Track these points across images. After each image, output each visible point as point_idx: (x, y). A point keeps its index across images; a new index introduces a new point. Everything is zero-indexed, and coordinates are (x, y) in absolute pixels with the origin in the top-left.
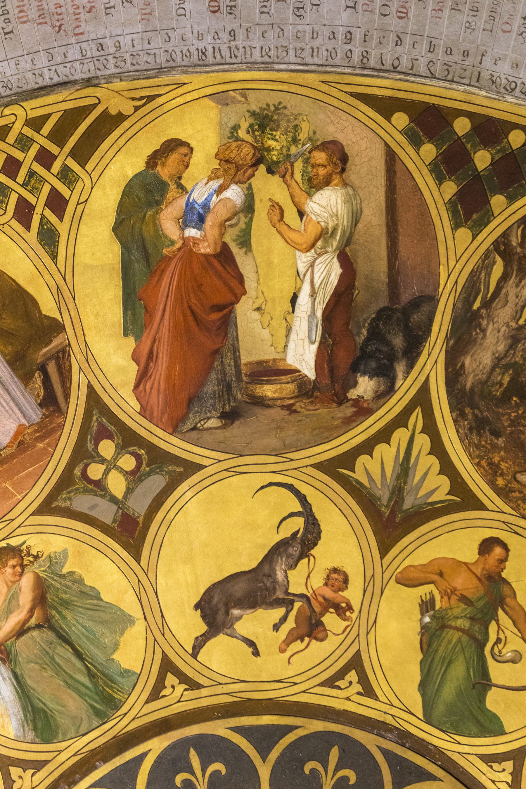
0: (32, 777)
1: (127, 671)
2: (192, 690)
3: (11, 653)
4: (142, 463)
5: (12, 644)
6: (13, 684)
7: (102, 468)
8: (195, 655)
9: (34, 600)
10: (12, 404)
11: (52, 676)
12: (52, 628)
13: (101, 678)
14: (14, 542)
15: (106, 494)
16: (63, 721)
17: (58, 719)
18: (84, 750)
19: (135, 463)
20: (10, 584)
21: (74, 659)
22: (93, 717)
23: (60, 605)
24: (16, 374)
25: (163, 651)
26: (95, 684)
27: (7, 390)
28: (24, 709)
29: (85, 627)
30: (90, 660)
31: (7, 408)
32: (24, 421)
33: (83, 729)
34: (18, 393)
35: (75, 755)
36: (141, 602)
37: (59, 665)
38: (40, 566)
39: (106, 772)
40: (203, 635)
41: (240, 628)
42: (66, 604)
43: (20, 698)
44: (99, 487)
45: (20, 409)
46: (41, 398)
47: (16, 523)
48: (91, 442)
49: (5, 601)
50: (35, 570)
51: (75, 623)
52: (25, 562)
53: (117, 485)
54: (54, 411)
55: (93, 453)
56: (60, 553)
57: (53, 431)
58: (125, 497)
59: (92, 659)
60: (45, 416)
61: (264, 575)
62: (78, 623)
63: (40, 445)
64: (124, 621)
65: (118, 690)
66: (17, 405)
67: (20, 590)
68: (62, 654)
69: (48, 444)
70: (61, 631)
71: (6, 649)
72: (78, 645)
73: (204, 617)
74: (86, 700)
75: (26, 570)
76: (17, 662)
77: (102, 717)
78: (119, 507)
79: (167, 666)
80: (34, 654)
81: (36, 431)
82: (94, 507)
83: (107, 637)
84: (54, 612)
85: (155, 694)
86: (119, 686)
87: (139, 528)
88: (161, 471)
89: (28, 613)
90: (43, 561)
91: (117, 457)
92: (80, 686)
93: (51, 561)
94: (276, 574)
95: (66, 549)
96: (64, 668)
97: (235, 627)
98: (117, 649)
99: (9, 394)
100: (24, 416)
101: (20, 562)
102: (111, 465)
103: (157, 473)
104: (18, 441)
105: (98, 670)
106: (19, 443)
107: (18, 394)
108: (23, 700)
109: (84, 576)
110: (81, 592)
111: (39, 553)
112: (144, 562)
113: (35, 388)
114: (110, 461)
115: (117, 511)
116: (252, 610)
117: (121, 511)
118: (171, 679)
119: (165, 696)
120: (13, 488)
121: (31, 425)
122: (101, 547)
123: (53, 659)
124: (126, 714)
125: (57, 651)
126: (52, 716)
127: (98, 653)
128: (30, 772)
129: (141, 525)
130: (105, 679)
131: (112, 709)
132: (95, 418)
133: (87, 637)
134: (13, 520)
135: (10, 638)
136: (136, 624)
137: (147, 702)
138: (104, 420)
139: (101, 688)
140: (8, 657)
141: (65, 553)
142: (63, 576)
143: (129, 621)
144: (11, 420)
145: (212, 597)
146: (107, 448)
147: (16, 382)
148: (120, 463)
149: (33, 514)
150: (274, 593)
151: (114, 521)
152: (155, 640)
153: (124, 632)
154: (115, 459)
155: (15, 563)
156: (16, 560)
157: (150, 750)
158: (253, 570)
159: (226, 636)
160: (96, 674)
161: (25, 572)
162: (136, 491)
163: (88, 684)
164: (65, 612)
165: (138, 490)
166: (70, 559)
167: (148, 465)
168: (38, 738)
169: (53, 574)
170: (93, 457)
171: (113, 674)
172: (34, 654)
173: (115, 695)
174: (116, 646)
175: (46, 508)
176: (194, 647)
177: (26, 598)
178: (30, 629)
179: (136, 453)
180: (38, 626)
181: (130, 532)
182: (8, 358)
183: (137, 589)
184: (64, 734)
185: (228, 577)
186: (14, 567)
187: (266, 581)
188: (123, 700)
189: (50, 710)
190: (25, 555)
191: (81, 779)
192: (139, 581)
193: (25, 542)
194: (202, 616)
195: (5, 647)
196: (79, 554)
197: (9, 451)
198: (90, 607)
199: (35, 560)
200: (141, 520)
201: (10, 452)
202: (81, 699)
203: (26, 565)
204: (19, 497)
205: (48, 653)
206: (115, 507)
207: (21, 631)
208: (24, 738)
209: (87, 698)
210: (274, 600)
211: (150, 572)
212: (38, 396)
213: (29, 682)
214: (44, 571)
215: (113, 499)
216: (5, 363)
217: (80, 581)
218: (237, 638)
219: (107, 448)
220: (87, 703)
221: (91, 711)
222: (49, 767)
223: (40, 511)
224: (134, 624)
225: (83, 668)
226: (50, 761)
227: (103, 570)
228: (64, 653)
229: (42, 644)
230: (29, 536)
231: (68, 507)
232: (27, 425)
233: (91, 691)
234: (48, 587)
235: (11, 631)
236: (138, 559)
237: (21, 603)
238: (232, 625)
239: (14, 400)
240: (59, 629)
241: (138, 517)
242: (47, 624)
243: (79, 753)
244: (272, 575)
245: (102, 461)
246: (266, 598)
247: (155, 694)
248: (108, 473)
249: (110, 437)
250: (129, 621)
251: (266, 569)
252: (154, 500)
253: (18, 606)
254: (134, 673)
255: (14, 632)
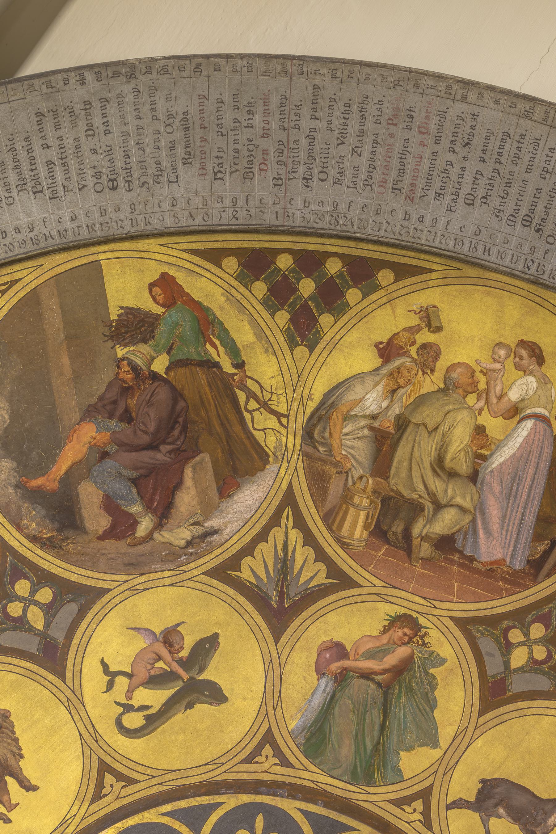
0: (274, 764)
1: (399, 770)
2: (424, 826)
3: (346, 680)
4: (547, 663)
5: (352, 676)
6: (326, 699)
7: (522, 638)
8: (449, 807)
9: (394, 667)
10: (513, 542)
11: (353, 722)
12: (386, 695)
13: (379, 757)
14: (422, 621)
15: (506, 655)
16: (329, 754)
17: (328, 750)
18: (321, 785)
19: (543, 658)
20: (391, 642)
21: (377, 727)
22: (349, 773)
23: (406, 687)
24: (534, 529)
25: (433, 784)
26: (372, 756)
27: (519, 531)
28: (316, 721)
29: (405, 717)
30: (385, 739)
31: (507, 541)
32: (508, 560)
33: (335, 773)
34: (524, 540)
35: (312, 781)
36: (453, 740)
37: (365, 720)
38: (420, 652)
39: (319, 813)
40: (468, 802)
41: (493, 822)
42: (410, 691)
43: (320, 713)
44: (507, 647)
45: (514, 551)
46: (534, 558)
47: (436, 612)
48: (532, 617)
49: (377, 647)
50: (415, 651)
51: (402, 708)
52: (414, 640)
53: (519, 658)
54: (532, 574)
55: (526, 624)
56: (441, 658)
57: (519, 585)
58: (516, 670)
59: (387, 739)
60: (523, 571)
61: (543, 809)
62: (404, 710)
63: (501, 584)
64: (432, 740)
65: (381, 775)
66: (515, 547)
67: (393, 652)
68: (373, 716)
69: (507, 589)
70: (388, 702)
71: (345, 675)
72: (389, 722)
73: (480, 792)
74: (356, 758)
75: (411, 644)
76: (343, 690)
77: (354, 779)
78: (505, 672)
79: (425, 795)
80: (358, 697)
81: (508, 573)
82: (490, 655)
83: (410, 737)
84: (397, 687)
85: (399, 803)
86: (384, 773)
87: (502, 697)
88: (552, 679)
89: (383, 670)
90: (426, 651)
91: (538, 642)
92: (363, 746)
93: (430, 656)
94: (550, 817)
95: (447, 660)
96: (366, 725)
97: (491, 818)
98: (409, 751)
99: (518, 535)
100: (512, 557)
101: (411, 636)
102: (529, 643)
103: (549, 679)
104: (492, 567)
105: (383, 750)
106: (491, 569)
107: (523, 541)
108: (320, 715)
109: (439, 686)
110: (427, 694)
111: (429, 644)
112: (482, 720)
113: (536, 549)
114: (531, 640)
115: (501, 673)
116: (512, 821)
117: (503, 675)
118: (418, 804)
119: (404, 811)
120: (457, 590)
121: (509, 567)
122: (468, 682)
123: (365, 713)
124: (370, 793)
125: (373, 711)
126: (326, 744)
127: (395, 740)
128: (276, 761)
129: (505, 697)
130: (382, 759)
131: (365, 781)
132: (550, 605)
133: (399, 723)
134: (436, 608)
135: (355, 672)
136: (436, 750)
137: (390, 801)
138: (555, 613)
139: (373, 761)
140: (342, 681)
141: (444, 661)
142: (426, 673)
143: (435, 744)
144: (501, 551)
145: (499, 787)
146: (537, 631)
147: (529, 532)
148: (535, 648)
149: (451, 618)
150: (537, 827)
151: (493, 677)
152: (436, 772)
153: (424, 746)
154: (535, 642)
155: (408, 633)
156: (411, 632)
157: (359, 830)
158: (541, 800)
159: (479, 818)
160: (379, 751)
161: (408, 645)
162: (526, 674)
163: (368, 751)
164: (404, 694)
165: (527, 675)
166: (442, 668)
167: (549, 668)
168: (303, 747)
169: (422, 664)
170: (523, 626)
171: (389, 762)
172: (358, 697)
173: (376, 776)
174: (409, 749)
175: (463, 623)
176: (454, 802)
177: (391, 660)
178: (373, 680)
179: (552, 653)
180: (379, 684)
181: (495, 693)
182: (541, 514)
183: (460, 730)
184: (321, 763)
185: (521, 786)
186: (405, 635)
187: (540, 813)
188: (378, 784)
189: (329, 739)
190: (419, 636)
191: (299, 800)
192: (467, 727)
193: (428, 628)
194: (479, 790)
195: (346, 673)
196: (451, 671)
197: (480, 566)
198: (422, 709)
199: (422, 645)
200: (509, 694)
201: (479, 567)
202: (354, 754)
203: (413, 642)
204: (455, 599)
205: (366, 706)
206: (502, 669)
207: (366, 675)
208: (296, 738)
209: (358, 758)
210: (532, 830)
211: (480, 730)
212: (533, 555)
213: (336, 709)
214: (419, 657)
215: (507, 664)
216: (536, 514)
217: (434, 687)
218: (485, 826)
219: (537, 631)
220: (355, 760)
221: (352, 768)
222: (290, 771)
223: (456, 621)
224: (435, 748)
225: (376, 739)
226: (295, 768)
227: (453, 698)
228: (376, 716)
229: (369, 696)
230: (435, 628)
231: (475, 638)
232: (508, 564)
233: (365, 757)
234: (411, 669)
235: (360, 669)
236: (481, 713)
237: (385, 659)
238: (491, 816)
239: (517, 540)
240: (389, 700)
241: (509, 691)
242: (386, 688)
243: (317, 783)
244: (547, 815)
245: (526, 634)
246: (528, 823)
247: (399, 803)
248: (522, 645)
249: (547, 627)
250: (435, 744)
251: (548, 807)
252: (529, 691)
253: (381, 660)
254: (402, 776)
255: (360, 671)
